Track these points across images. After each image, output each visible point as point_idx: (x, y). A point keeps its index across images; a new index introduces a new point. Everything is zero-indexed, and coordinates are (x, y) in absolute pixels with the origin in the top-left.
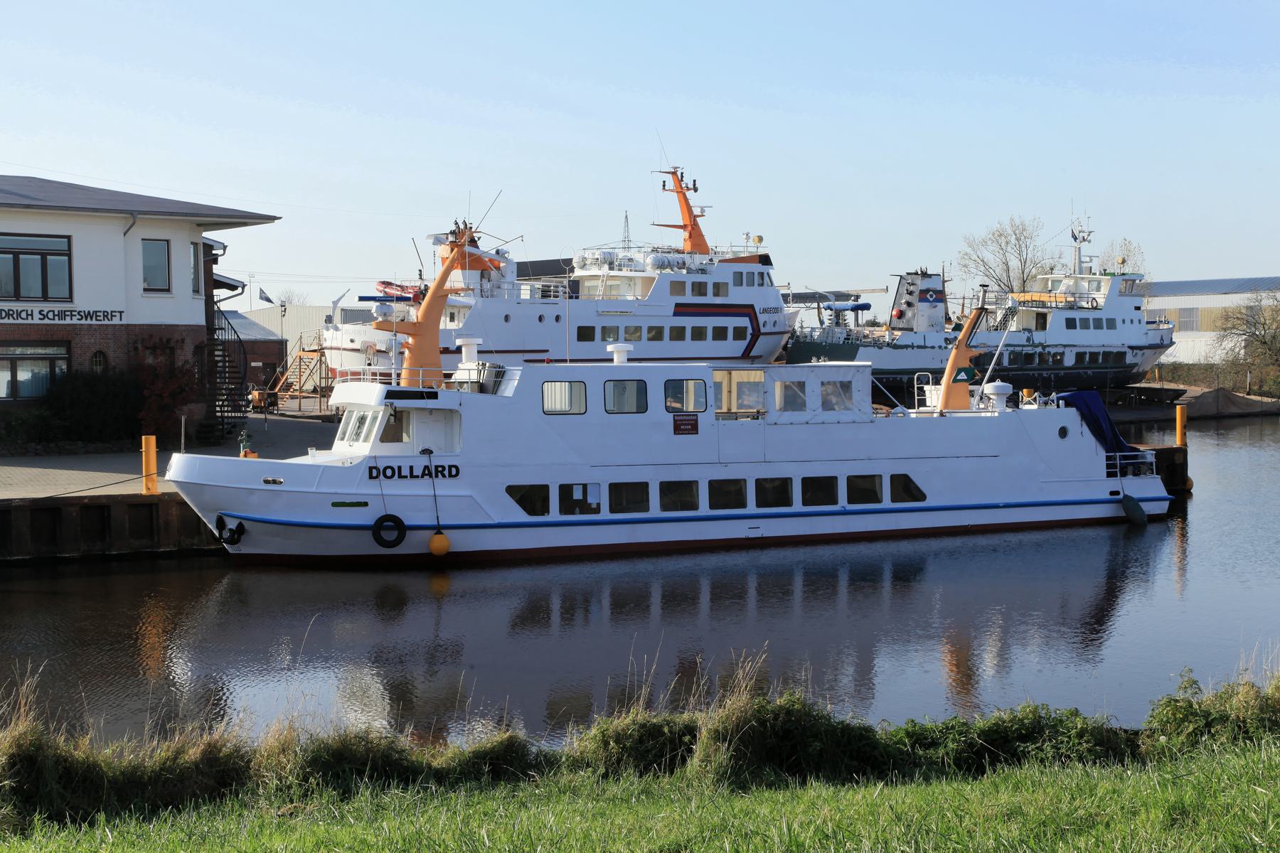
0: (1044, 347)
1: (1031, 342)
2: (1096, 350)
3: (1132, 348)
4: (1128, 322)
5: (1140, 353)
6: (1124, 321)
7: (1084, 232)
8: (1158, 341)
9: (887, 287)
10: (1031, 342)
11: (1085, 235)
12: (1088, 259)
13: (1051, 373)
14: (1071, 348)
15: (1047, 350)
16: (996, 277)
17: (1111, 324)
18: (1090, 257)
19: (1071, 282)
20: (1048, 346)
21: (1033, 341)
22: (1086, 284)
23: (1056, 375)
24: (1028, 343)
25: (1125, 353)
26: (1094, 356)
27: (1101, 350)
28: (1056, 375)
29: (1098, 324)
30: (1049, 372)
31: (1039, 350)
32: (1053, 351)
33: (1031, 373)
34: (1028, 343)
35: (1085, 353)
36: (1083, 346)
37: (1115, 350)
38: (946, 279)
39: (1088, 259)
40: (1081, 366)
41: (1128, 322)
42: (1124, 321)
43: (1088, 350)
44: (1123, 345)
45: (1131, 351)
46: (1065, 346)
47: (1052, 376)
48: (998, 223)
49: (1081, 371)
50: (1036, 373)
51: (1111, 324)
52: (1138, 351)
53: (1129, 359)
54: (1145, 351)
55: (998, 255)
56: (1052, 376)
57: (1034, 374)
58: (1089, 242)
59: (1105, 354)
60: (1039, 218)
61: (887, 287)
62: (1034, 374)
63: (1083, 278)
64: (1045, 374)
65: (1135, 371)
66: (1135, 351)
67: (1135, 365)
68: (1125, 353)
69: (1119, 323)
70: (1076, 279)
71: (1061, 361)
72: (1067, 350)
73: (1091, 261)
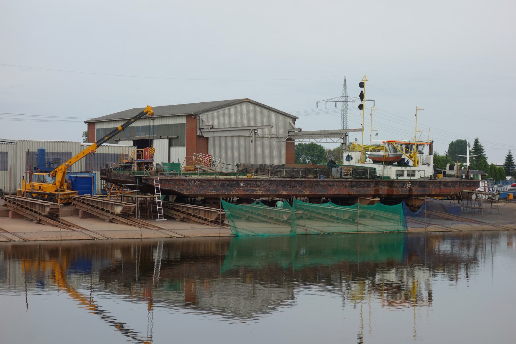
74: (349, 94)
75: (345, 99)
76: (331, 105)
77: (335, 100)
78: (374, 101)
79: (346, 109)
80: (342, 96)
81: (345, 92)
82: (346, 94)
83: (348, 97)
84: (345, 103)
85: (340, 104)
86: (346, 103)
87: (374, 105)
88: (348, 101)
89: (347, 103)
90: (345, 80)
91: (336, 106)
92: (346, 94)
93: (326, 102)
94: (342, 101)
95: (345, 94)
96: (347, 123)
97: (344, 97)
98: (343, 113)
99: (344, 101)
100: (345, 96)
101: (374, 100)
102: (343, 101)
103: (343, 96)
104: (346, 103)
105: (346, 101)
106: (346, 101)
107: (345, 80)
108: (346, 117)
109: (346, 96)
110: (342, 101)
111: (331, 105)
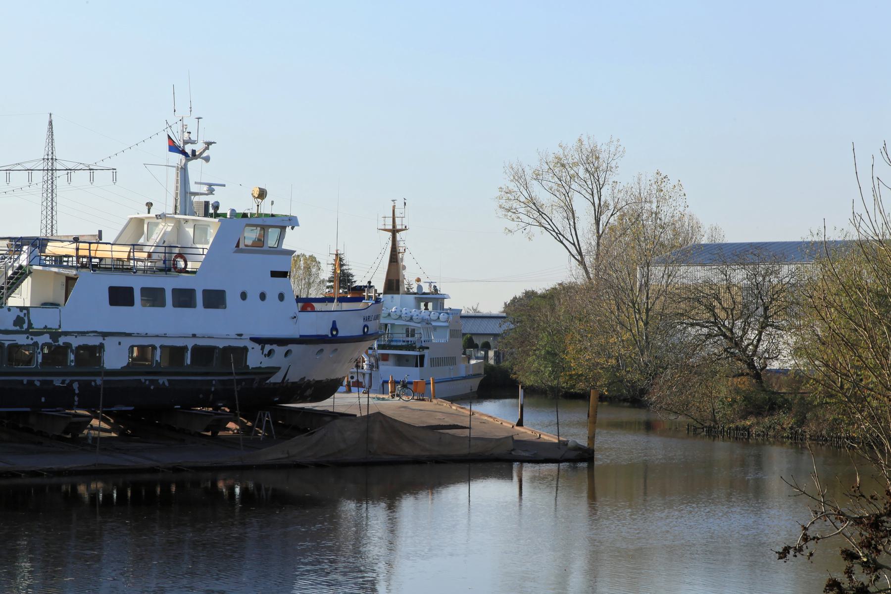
0: (55, 335)
1: (25, 326)
2: (179, 343)
3: (255, 340)
4: (254, 296)
5: (280, 350)
6: (244, 296)
7: (193, 142)
8: (325, 331)
9: (100, 232)
10: (25, 326)
11: (199, 148)
12: (204, 189)
13: (72, 382)
14: (116, 339)
15: (62, 340)
16: (557, 231)
17: (215, 299)
18: (210, 185)
19: (169, 227)
20: (66, 334)
21: (30, 325)
22: (190, 231)
23: (84, 386)
24: (18, 328)
25: (245, 350)
26: (175, 353)
27: (190, 343)
28: (84, 386)
29: (184, 298)
30: (68, 379)
31: (46, 339)
32: (75, 342)
33: (25, 379)
34: (18, 328)
35: (184, 349)
36: (146, 336)
37: (221, 344)
38: (398, 227)
39: (204, 189)
40: (59, 368)
41: (254, 296)
42: (244, 296)
43: (158, 343)
44: (241, 335)
45: (258, 347)
46: (105, 335)
47: (76, 386)
48: (560, 146)
49: (142, 378)
50: (37, 381)
51: (215, 299)
52: (275, 347)
53: (255, 359)
54: (290, 347)
55: (558, 194)
56: (76, 386)
57: (31, 383)
58: (207, 159)
59: (197, 350)
60: (618, 141)
61: (100, 232)
62: (31, 383)
63: (187, 221)
64: (57, 381)
65: (306, 380)
66: (268, 348)
67: (273, 371)
68: (245, 350)
69: (232, 298)
70: (179, 220)
71: (99, 360)
72: (110, 343)
73: (211, 192)
74: (57, 155)
75: (50, 164)
76: (18, 178)
77: (28, 166)
78: (114, 171)
79: (52, 187)
80: (44, 159)
81: (50, 149)
82: (52, 153)
83: (56, 159)
84: (50, 174)
85: (38, 177)
86: (52, 174)
87: (115, 180)
88: (56, 170)
89: (55, 174)
90: (51, 123)
91: (30, 180)
92: (52, 153)
93: (6, 170)
94: (44, 170)
95: (50, 153)
96: (55, 218)
97: (48, 159)
98: (45, 195)
99: (48, 170)
100: (50, 157)
101: (115, 169)
102: (46, 168)
103: (46, 157)
104: (52, 174)
105: (52, 170)
106: (52, 170)
107: (51, 123)
108: (52, 204)
109: (52, 159)
110: (44, 170)
111: (18, 178)
